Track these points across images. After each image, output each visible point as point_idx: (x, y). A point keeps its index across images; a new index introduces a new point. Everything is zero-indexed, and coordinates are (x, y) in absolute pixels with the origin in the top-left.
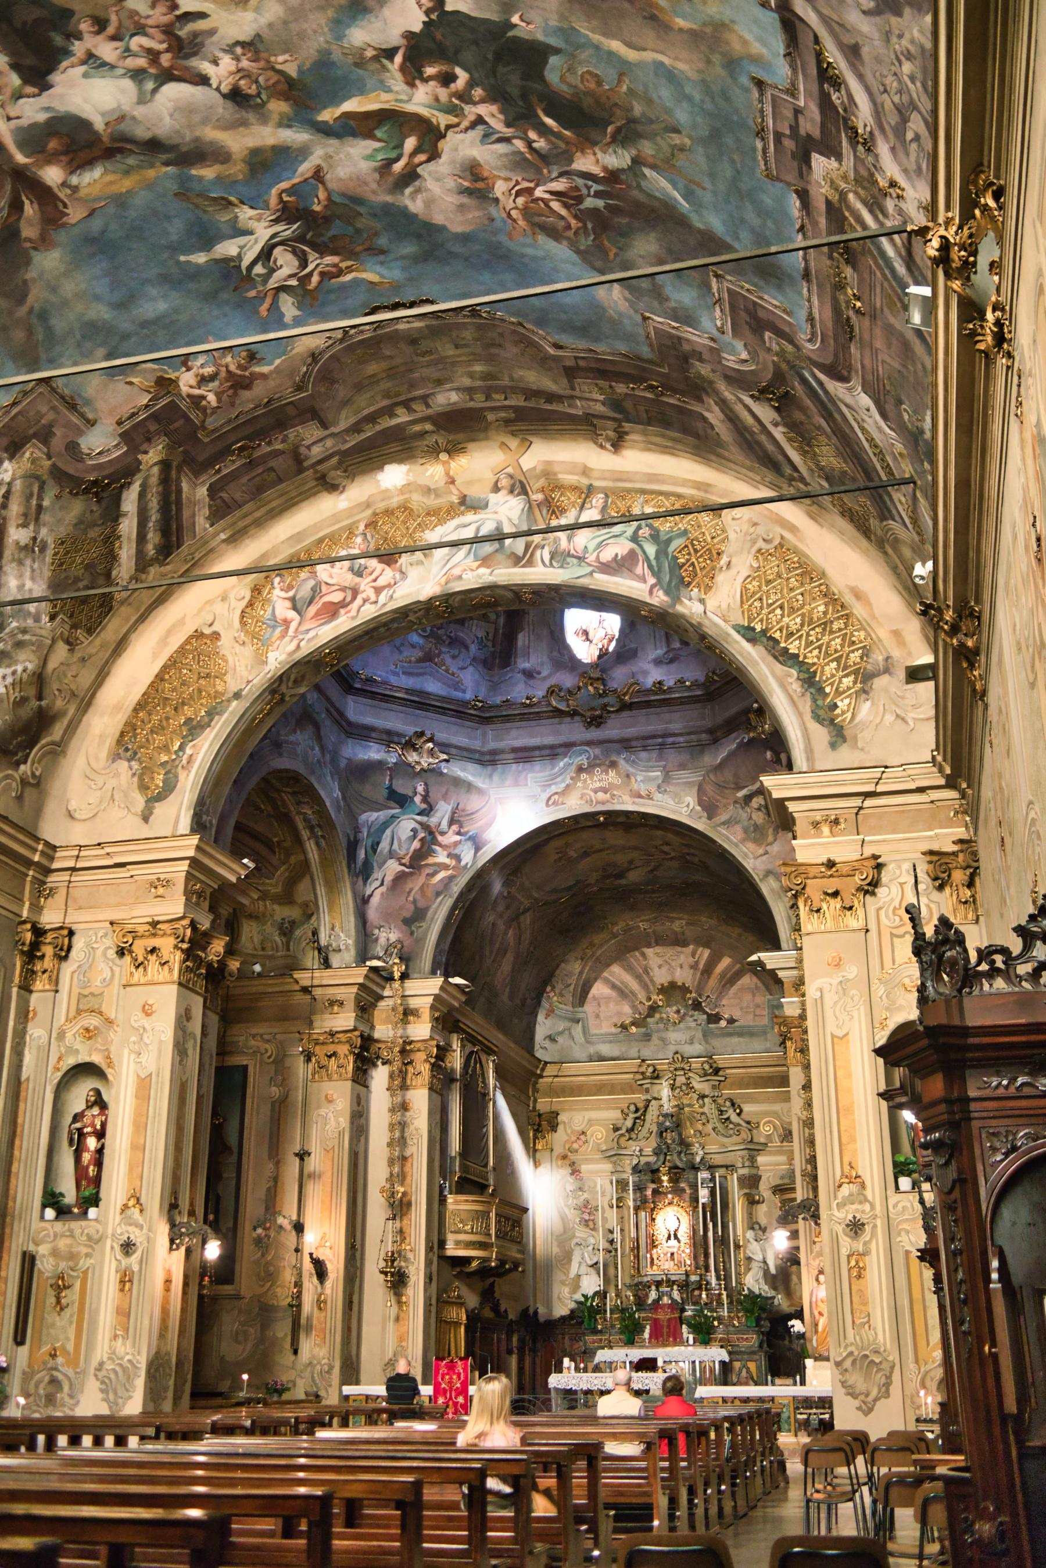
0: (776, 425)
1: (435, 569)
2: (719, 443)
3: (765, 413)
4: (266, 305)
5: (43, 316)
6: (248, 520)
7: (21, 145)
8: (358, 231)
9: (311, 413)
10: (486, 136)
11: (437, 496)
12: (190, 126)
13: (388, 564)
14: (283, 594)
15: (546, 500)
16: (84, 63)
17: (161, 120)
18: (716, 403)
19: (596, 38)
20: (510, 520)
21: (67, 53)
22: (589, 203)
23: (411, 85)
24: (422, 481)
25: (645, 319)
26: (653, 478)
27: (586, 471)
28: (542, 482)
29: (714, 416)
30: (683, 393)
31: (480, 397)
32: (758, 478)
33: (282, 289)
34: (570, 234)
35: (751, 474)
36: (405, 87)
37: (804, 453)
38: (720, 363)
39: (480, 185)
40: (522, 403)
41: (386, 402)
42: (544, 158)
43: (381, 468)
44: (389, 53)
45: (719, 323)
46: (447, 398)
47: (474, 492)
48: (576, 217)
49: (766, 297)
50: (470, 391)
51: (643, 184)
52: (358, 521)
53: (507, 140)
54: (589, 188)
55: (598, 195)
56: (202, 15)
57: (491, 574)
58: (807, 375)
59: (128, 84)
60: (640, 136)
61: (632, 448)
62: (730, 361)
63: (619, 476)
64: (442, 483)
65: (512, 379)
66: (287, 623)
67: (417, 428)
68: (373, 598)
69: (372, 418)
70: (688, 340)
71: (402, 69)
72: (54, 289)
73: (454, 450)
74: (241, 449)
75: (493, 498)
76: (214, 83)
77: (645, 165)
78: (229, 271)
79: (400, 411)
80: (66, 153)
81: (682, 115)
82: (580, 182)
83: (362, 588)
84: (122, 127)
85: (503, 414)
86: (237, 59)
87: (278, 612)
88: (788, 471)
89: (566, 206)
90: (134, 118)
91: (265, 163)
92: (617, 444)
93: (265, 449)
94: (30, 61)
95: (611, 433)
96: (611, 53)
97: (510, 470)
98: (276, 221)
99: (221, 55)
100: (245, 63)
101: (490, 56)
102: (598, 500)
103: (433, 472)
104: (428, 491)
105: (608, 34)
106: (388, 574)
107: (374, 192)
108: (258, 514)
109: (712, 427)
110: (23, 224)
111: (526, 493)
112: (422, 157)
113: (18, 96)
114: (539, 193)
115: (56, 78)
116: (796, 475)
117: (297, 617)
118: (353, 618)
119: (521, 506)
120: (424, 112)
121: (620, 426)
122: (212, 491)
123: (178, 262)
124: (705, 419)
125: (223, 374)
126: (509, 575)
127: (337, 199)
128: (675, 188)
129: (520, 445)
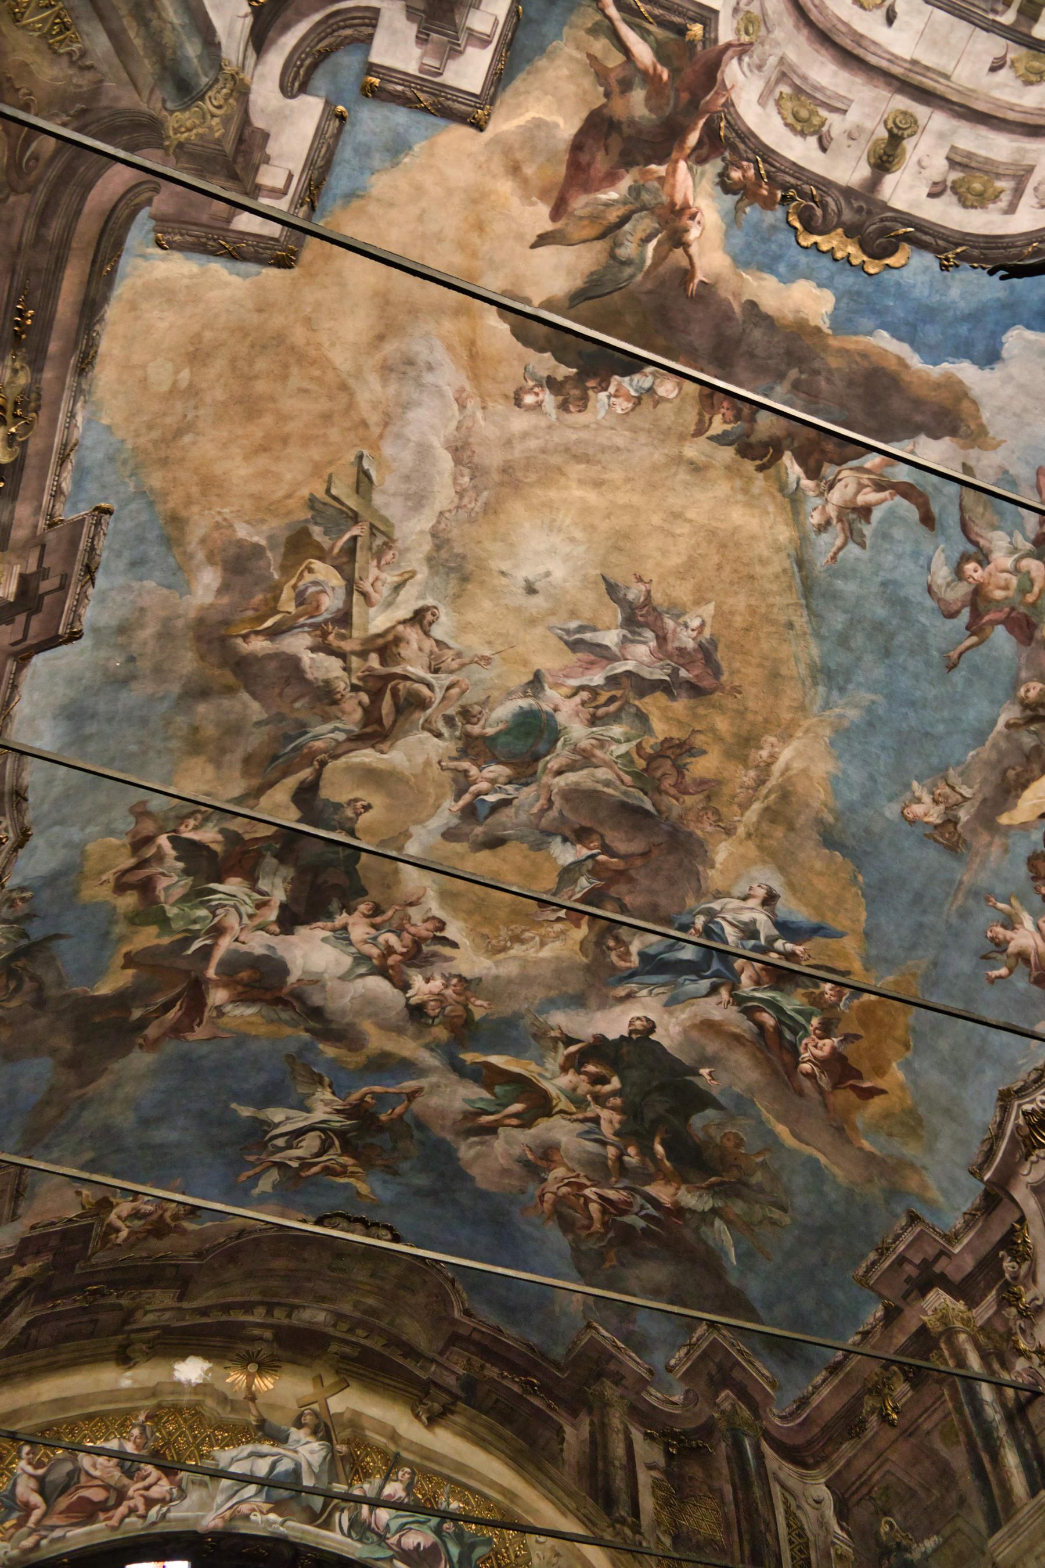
0: (650, 1467)
1: (219, 1499)
2: (556, 1459)
3: (648, 1452)
4: (251, 1173)
5: (84, 1104)
6: (25, 1366)
7: (222, 963)
8: (394, 1149)
9: (182, 1282)
10: (588, 1132)
11: (234, 1410)
12: (358, 1013)
13: (167, 1475)
14: (30, 1469)
15: (352, 1451)
16: (334, 930)
17: (342, 997)
18: (592, 1424)
19: (766, 1115)
20: (310, 1465)
21: (330, 917)
22: (630, 1219)
23: (564, 1069)
24: (219, 1386)
25: (589, 1326)
26: (461, 1467)
27: (394, 1436)
28: (346, 1433)
29: (575, 1435)
30: (557, 1399)
31: (345, 1327)
32: (573, 1505)
33: (281, 1166)
34: (584, 1233)
35: (566, 1500)
36: (557, 1069)
37: (664, 1503)
38: (638, 1393)
39: (543, 1164)
40: (378, 1348)
41: (255, 1297)
42: (623, 1169)
43: (183, 1357)
44: (569, 1041)
45: (673, 1362)
46: (315, 1316)
47: (276, 1419)
48: (604, 1224)
49: (757, 1364)
50: (340, 1317)
51: (704, 1229)
52: (137, 1409)
53: (604, 1143)
54: (642, 1208)
55: (647, 1217)
56: (454, 945)
57: (282, 1524)
58: (747, 1442)
59: (347, 961)
60: (739, 1195)
61: (446, 1427)
62: (654, 1396)
63: (428, 1454)
64: (241, 1396)
65: (392, 1323)
66: (28, 1508)
67: (257, 1332)
68: (142, 1510)
69: (226, 1308)
70: (620, 1362)
71: (569, 1057)
72: (117, 1085)
73: (266, 1366)
74: (93, 1293)
75: (295, 1434)
76: (410, 993)
77: (721, 1217)
78: (258, 1134)
79: (261, 1311)
80: (245, 985)
81: (801, 1201)
82: (639, 1200)
83: (130, 1493)
84: (309, 989)
85: (347, 1350)
86: (446, 986)
87: (20, 1490)
88: (623, 1512)
89: (604, 1211)
90: (324, 986)
91: (384, 1065)
92: (432, 1421)
93: (112, 1300)
94: (299, 909)
95: (437, 1407)
96: (771, 1132)
97: (316, 1407)
98: (338, 1112)
99: (438, 977)
100: (449, 992)
101: (655, 1083)
102: (404, 1473)
103: (236, 1379)
104: (224, 1399)
105: (782, 1119)
106: (163, 1488)
107: (443, 1127)
108: (40, 1363)
109: (562, 1440)
110: (156, 1022)
111: (330, 1440)
112: (514, 1122)
113: (262, 928)
114: (587, 1192)
115: (303, 931)
116: (630, 1519)
117: (43, 1507)
118: (114, 1529)
119: (323, 1453)
120: (553, 1091)
121: (454, 1404)
122: (30, 1324)
123: (227, 1107)
124: (560, 1431)
125: (155, 1217)
126: (304, 1532)
127: (407, 1118)
128: (735, 1246)
129: (335, 1384)
